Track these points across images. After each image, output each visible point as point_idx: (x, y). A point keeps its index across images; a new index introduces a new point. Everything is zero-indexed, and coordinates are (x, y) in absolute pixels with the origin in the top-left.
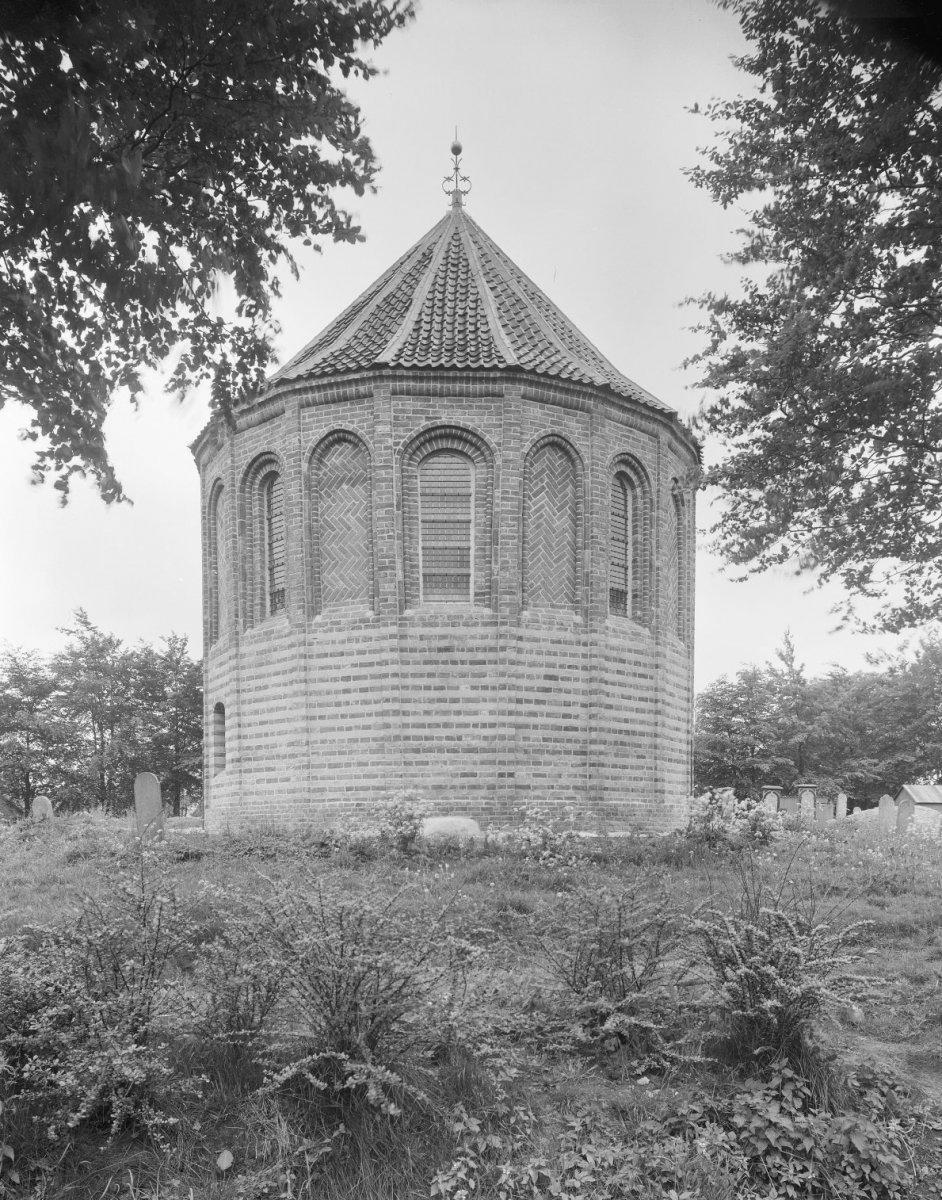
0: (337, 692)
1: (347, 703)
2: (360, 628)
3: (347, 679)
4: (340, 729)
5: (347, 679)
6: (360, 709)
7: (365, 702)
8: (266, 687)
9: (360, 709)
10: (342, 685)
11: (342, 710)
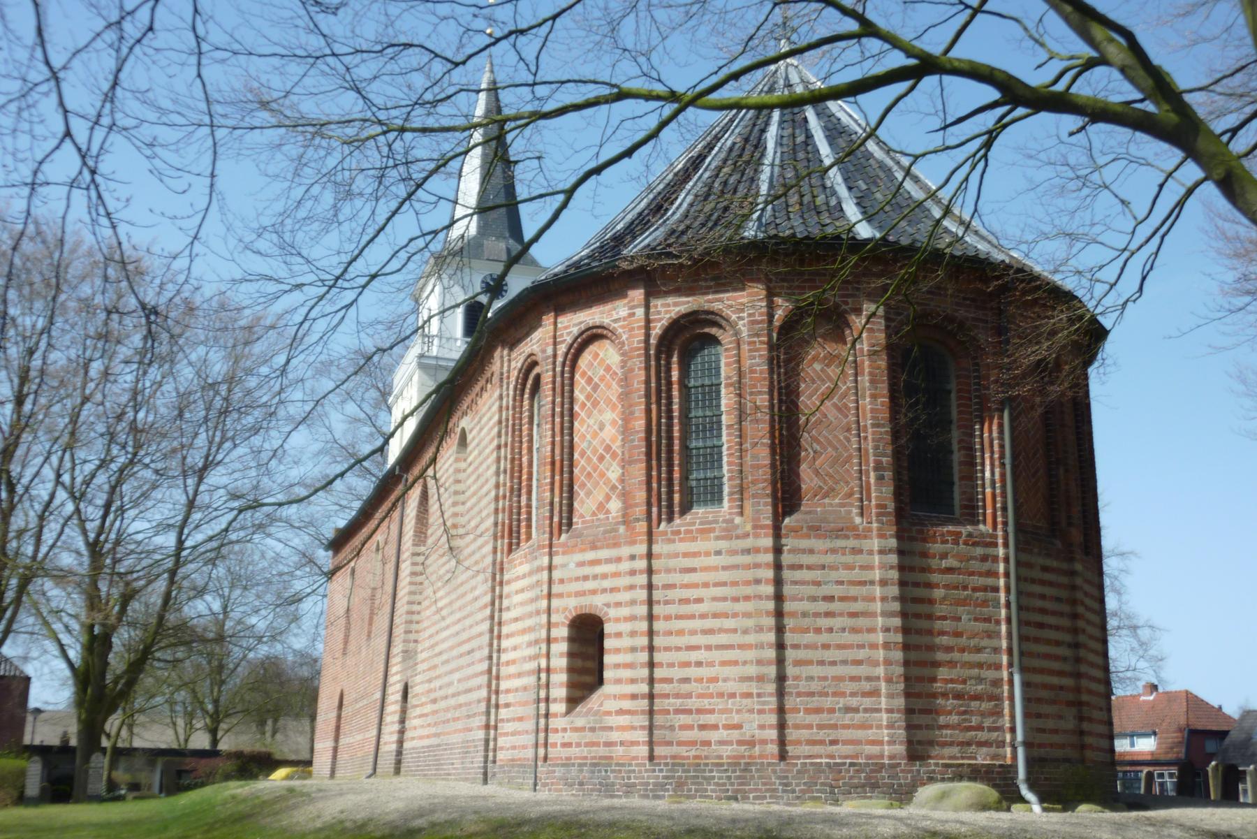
0: (817, 615)
1: (830, 630)
2: (847, 537)
3: (829, 599)
5: (829, 599)
6: (847, 638)
7: (854, 630)
8: (699, 600)
9: (847, 638)
10: (823, 607)
11: (824, 638)
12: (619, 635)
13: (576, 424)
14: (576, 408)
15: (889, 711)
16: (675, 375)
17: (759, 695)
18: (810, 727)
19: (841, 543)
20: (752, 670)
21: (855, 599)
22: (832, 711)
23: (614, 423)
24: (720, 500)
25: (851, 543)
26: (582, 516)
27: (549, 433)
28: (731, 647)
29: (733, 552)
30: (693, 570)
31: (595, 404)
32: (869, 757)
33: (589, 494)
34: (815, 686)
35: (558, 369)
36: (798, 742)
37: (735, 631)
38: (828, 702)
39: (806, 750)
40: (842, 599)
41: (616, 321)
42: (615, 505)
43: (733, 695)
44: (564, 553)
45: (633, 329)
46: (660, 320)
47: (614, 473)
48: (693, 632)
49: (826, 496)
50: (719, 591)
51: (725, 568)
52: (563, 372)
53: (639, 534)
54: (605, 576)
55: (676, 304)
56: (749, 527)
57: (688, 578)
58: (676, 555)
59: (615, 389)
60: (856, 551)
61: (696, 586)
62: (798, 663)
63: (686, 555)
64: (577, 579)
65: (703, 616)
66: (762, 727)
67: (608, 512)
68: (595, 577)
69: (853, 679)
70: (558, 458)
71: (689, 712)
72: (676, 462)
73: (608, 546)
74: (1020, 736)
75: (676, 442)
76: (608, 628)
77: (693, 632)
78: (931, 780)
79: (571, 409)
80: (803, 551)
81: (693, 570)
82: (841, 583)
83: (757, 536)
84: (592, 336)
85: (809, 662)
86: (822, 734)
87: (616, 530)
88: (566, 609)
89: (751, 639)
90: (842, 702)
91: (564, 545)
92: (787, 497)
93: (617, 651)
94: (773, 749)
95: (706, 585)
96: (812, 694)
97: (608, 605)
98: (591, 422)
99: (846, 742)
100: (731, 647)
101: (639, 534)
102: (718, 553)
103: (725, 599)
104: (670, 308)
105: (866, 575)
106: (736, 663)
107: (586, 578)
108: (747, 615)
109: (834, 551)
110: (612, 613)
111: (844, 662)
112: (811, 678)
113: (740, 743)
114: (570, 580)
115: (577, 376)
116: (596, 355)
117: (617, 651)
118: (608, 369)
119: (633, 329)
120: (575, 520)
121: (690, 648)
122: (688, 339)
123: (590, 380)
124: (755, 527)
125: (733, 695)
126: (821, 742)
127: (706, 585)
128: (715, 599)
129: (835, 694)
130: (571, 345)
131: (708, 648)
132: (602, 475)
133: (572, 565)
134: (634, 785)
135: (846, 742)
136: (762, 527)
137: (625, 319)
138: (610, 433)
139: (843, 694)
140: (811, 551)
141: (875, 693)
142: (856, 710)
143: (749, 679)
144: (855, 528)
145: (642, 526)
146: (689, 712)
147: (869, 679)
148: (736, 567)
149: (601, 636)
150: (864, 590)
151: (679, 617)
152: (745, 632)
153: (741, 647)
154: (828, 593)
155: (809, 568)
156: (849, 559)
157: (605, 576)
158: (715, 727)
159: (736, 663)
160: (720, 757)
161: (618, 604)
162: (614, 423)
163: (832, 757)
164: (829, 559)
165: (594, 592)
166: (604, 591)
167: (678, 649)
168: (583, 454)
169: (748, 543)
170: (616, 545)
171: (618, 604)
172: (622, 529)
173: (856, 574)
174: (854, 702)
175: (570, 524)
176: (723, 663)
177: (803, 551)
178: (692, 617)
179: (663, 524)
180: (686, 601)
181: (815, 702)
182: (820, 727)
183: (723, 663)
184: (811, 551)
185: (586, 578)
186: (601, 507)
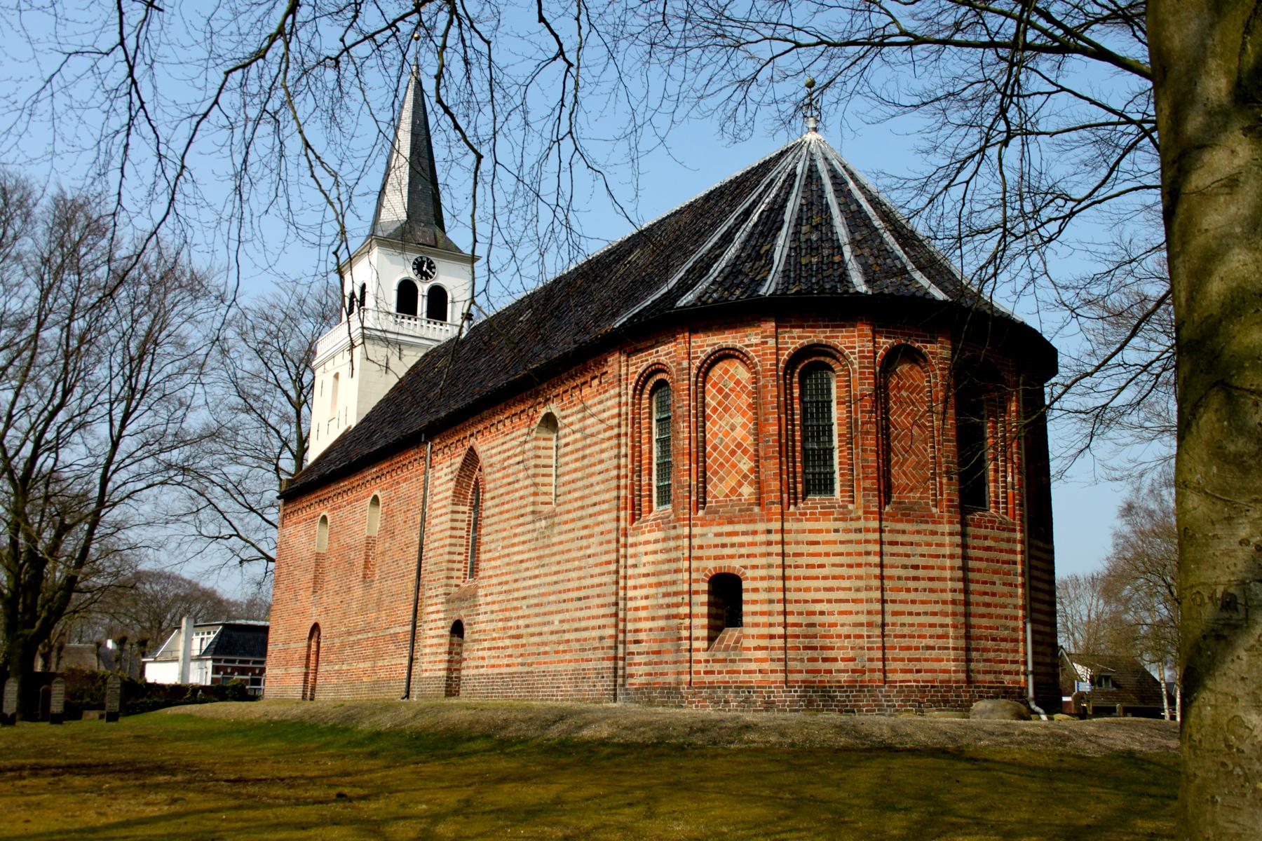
0: (907, 579)
1: (916, 590)
2: (927, 522)
3: (915, 567)
4: (910, 614)
5: (915, 567)
7: (932, 591)
8: (822, 566)
10: (912, 573)
11: (912, 596)
12: (756, 590)
13: (708, 424)
14: (708, 411)
15: (955, 649)
16: (796, 392)
17: (869, 637)
18: (902, 660)
19: (923, 527)
20: (863, 619)
21: (932, 568)
22: (917, 648)
23: (744, 426)
24: (832, 491)
25: (930, 527)
26: (715, 497)
27: (687, 430)
28: (847, 601)
29: (847, 531)
30: (817, 543)
31: (726, 409)
32: (941, 682)
33: (721, 480)
34: (906, 631)
35: (693, 379)
36: (895, 671)
37: (850, 589)
38: (915, 642)
39: (900, 676)
40: (925, 567)
41: (747, 346)
42: (747, 491)
43: (848, 637)
44: (702, 526)
45: (765, 354)
46: (787, 349)
47: (746, 465)
48: (817, 590)
49: (911, 490)
50: (837, 560)
51: (842, 542)
52: (696, 382)
53: (775, 514)
54: (742, 545)
55: (800, 338)
56: (860, 513)
57: (813, 549)
58: (804, 531)
59: (745, 401)
60: (934, 533)
61: (819, 555)
62: (895, 614)
63: (811, 531)
64: (716, 546)
65: (825, 578)
66: (871, 660)
67: (740, 495)
68: (733, 545)
69: (931, 625)
70: (693, 450)
71: (815, 648)
72: (798, 460)
73: (744, 522)
74: (1030, 668)
75: (798, 444)
76: (745, 585)
77: (817, 590)
78: (981, 697)
79: (704, 412)
80: (898, 532)
81: (817, 543)
82: (923, 556)
83: (866, 519)
84: (724, 355)
85: (902, 613)
86: (911, 666)
87: (751, 510)
88: (705, 569)
89: (863, 595)
90: (924, 642)
91: (701, 519)
92: (885, 490)
93: (755, 602)
94: (878, 675)
95: (827, 555)
96: (904, 636)
97: (745, 567)
98: (722, 423)
99: (927, 671)
100: (847, 601)
101: (775, 514)
102: (836, 531)
103: (842, 565)
104: (795, 339)
105: (941, 551)
106: (850, 613)
107: (724, 546)
108: (859, 578)
109: (918, 532)
110: (749, 573)
111: (926, 613)
112: (903, 625)
113: (854, 671)
114: (709, 547)
115: (708, 386)
116: (726, 371)
117: (755, 602)
118: (738, 382)
119: (765, 354)
120: (708, 499)
121: (815, 601)
122: (810, 366)
123: (720, 391)
124: (865, 513)
125: (848, 637)
126: (910, 671)
127: (827, 555)
128: (834, 565)
129: (919, 637)
130: (705, 361)
131: (829, 601)
132: (734, 466)
133: (711, 535)
134: (773, 702)
135: (927, 671)
136: (872, 513)
137: (756, 345)
138: (739, 433)
139: (924, 637)
140: (904, 532)
141: (945, 636)
142: (933, 648)
143: (861, 625)
144: (932, 516)
145: (776, 508)
146: (815, 648)
147: (942, 626)
148: (850, 542)
149: (739, 590)
150: (938, 562)
151: (806, 578)
152: (858, 590)
153: (854, 601)
154: (915, 563)
155: (902, 544)
156: (929, 538)
157: (742, 545)
158: (835, 660)
159: (850, 613)
160: (839, 682)
161: (754, 567)
162: (744, 426)
163: (917, 681)
164: (916, 538)
165: (732, 557)
166: (741, 556)
167: (806, 601)
168: (715, 448)
169: (861, 524)
170: (752, 521)
171: (754, 567)
172: (756, 509)
173: (933, 550)
174: (931, 642)
175: (705, 503)
176: (841, 613)
177: (898, 532)
178: (817, 578)
179: (792, 507)
180: (812, 566)
181: (906, 642)
182: (910, 660)
183: (841, 613)
184: (904, 532)
185: (724, 546)
186: (733, 490)
